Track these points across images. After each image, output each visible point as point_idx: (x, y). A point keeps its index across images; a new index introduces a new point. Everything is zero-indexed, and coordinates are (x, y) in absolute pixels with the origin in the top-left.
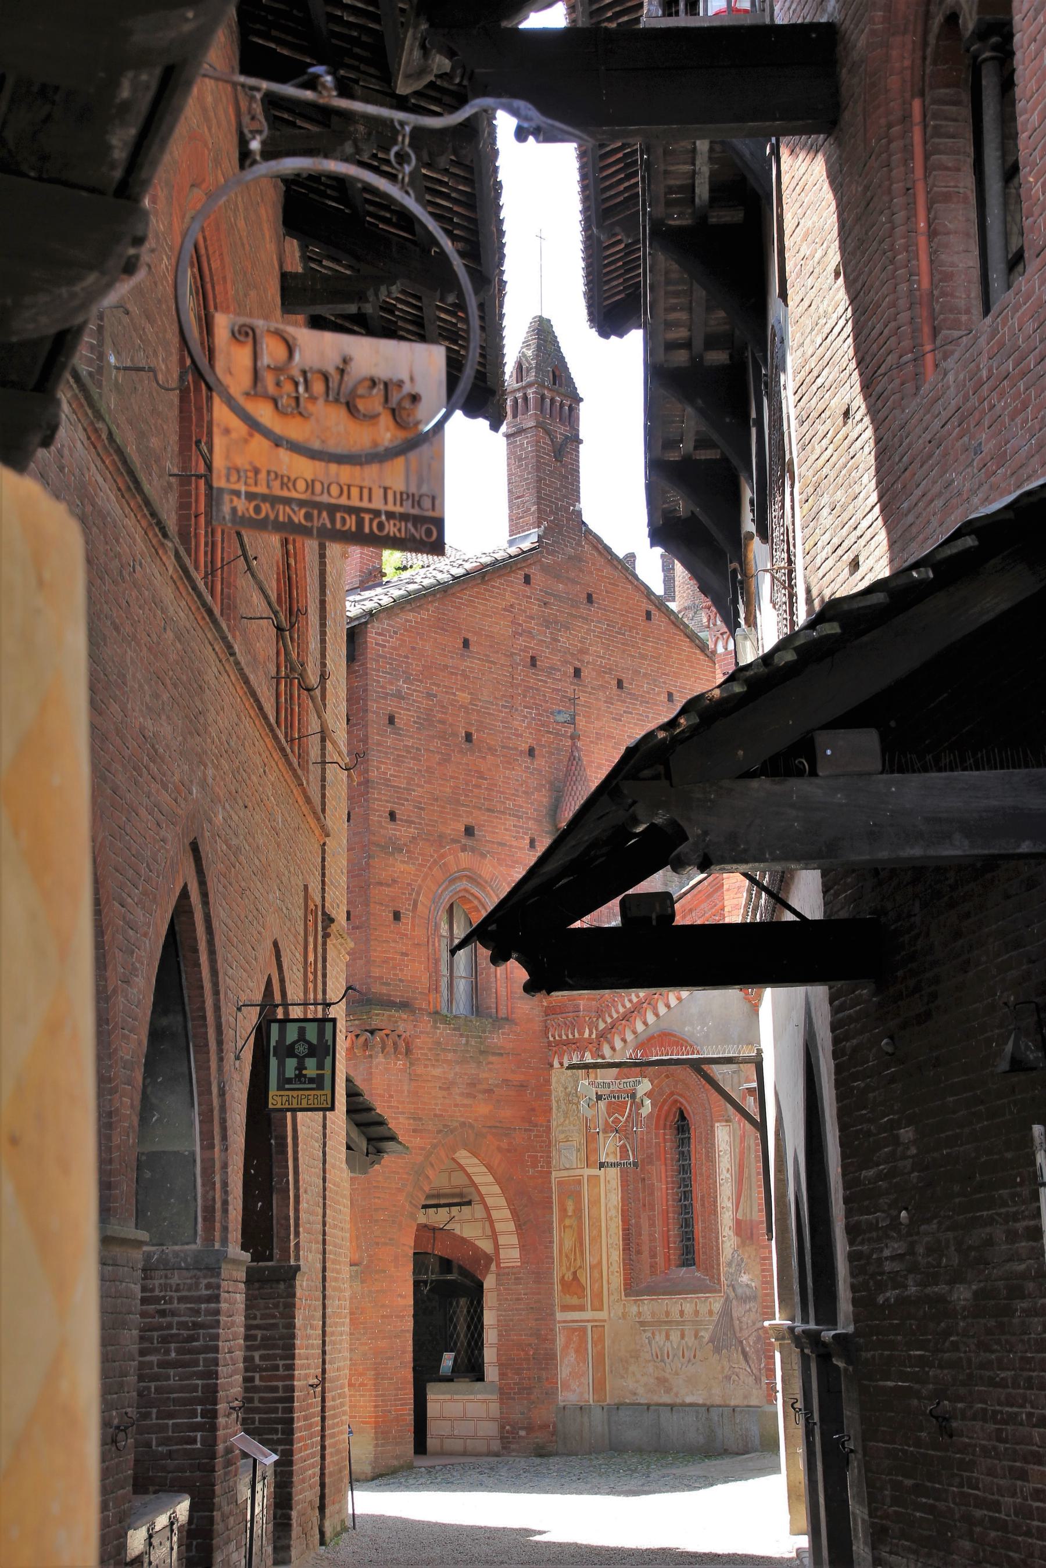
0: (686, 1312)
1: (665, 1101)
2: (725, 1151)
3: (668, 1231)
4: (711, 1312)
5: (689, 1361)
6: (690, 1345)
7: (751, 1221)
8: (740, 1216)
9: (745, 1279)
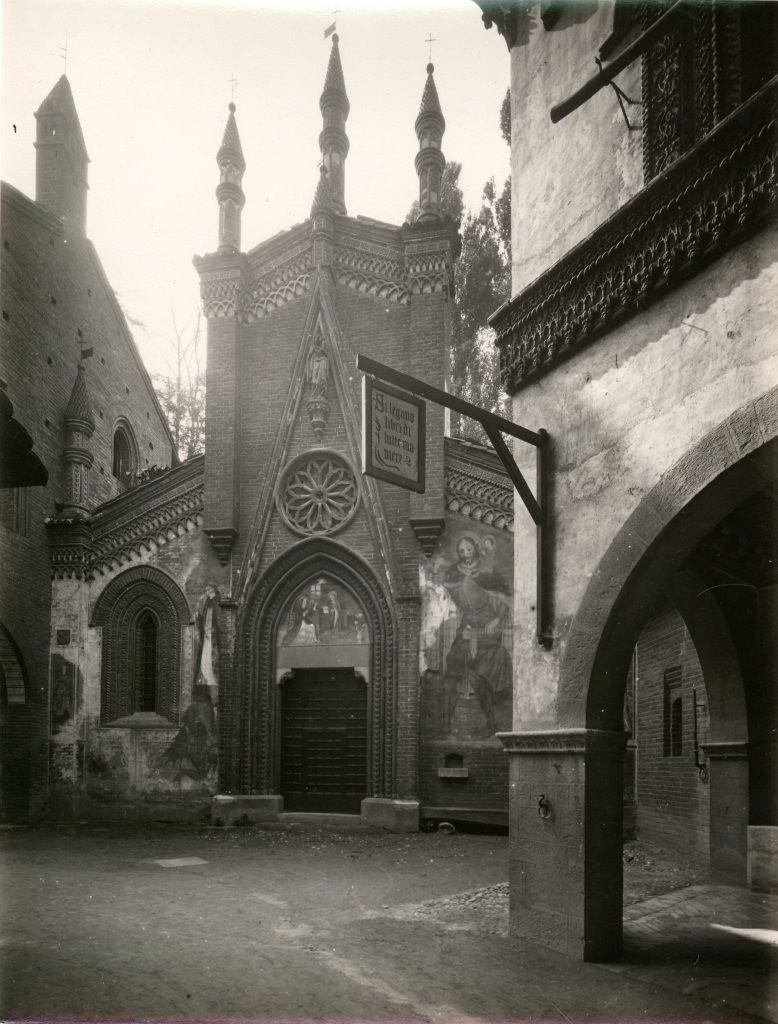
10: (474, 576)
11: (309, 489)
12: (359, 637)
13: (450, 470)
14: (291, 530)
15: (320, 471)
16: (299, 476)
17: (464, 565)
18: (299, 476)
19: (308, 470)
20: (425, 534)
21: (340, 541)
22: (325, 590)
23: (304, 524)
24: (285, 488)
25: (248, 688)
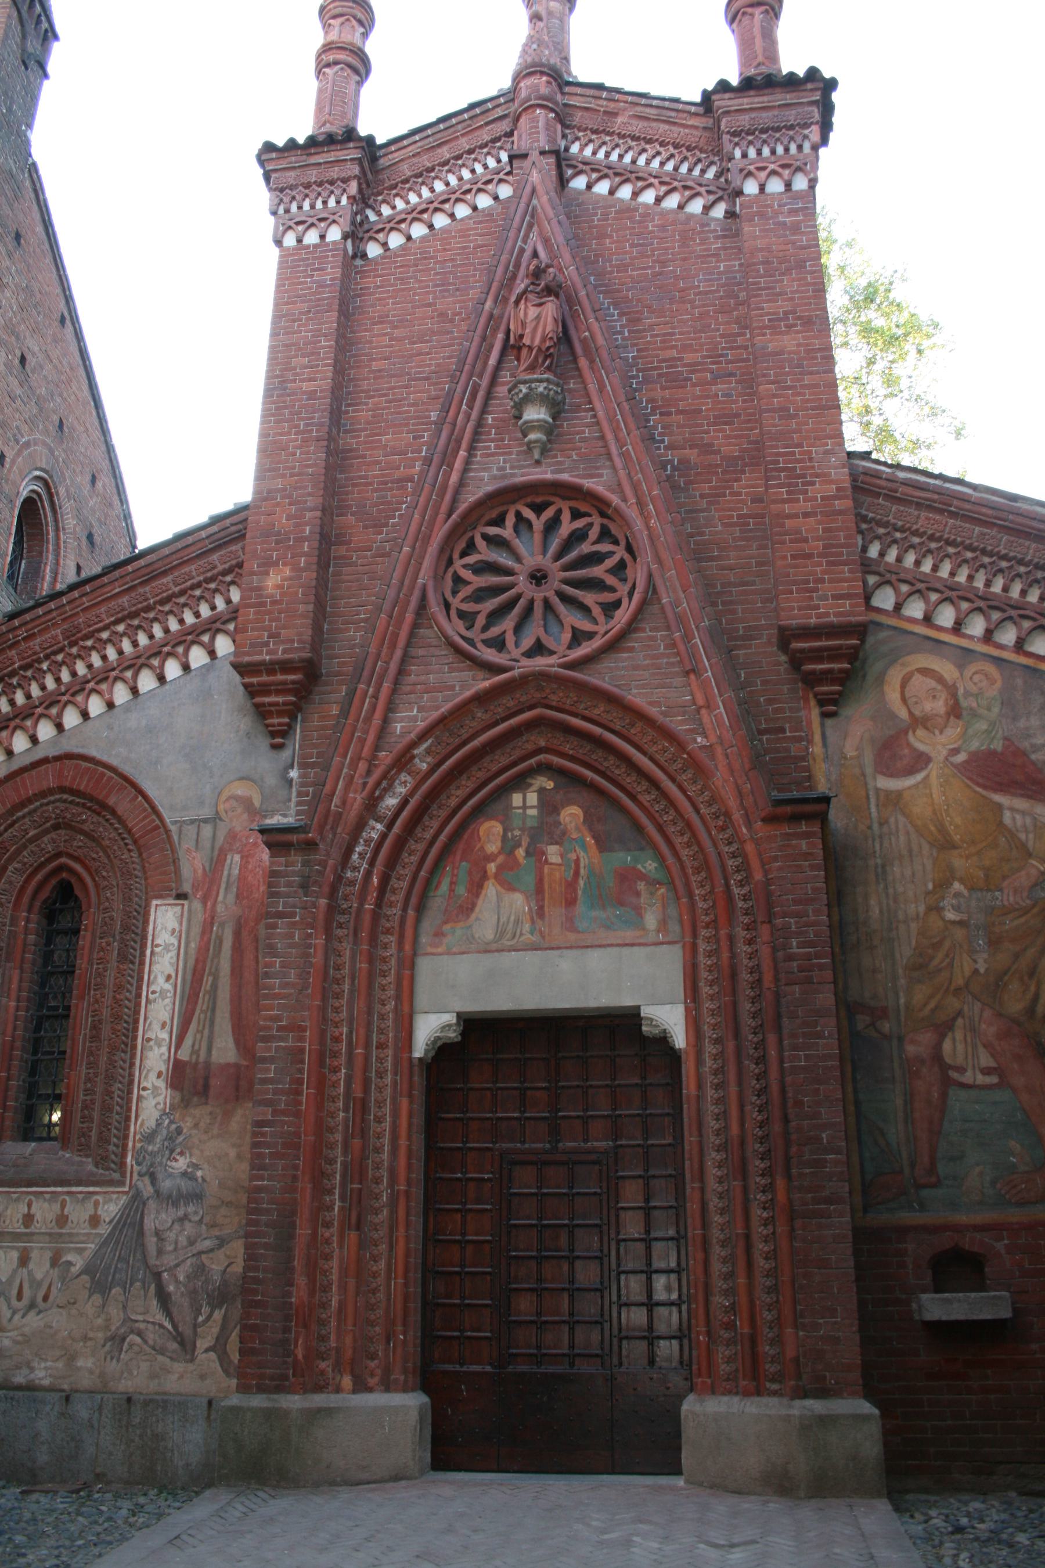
0: (38, 1216)
1: (42, 865)
2: (167, 948)
3: (8, 1079)
4: (94, 1221)
5: (32, 1305)
6: (39, 1276)
7: (207, 1064)
8: (184, 1055)
9: (181, 1164)
10: (961, 757)
11: (516, 566)
12: (651, 920)
13: (864, 519)
14: (458, 650)
15: (538, 524)
16: (485, 537)
17: (920, 732)
18: (485, 537)
19: (510, 520)
20: (820, 660)
21: (595, 678)
22: (549, 806)
23: (499, 644)
24: (450, 562)
25: (336, 1070)
